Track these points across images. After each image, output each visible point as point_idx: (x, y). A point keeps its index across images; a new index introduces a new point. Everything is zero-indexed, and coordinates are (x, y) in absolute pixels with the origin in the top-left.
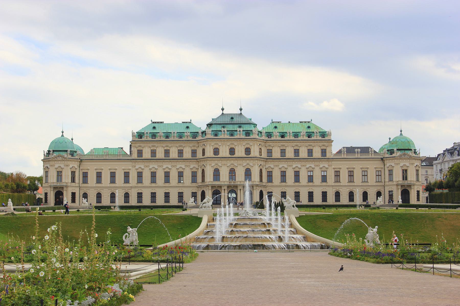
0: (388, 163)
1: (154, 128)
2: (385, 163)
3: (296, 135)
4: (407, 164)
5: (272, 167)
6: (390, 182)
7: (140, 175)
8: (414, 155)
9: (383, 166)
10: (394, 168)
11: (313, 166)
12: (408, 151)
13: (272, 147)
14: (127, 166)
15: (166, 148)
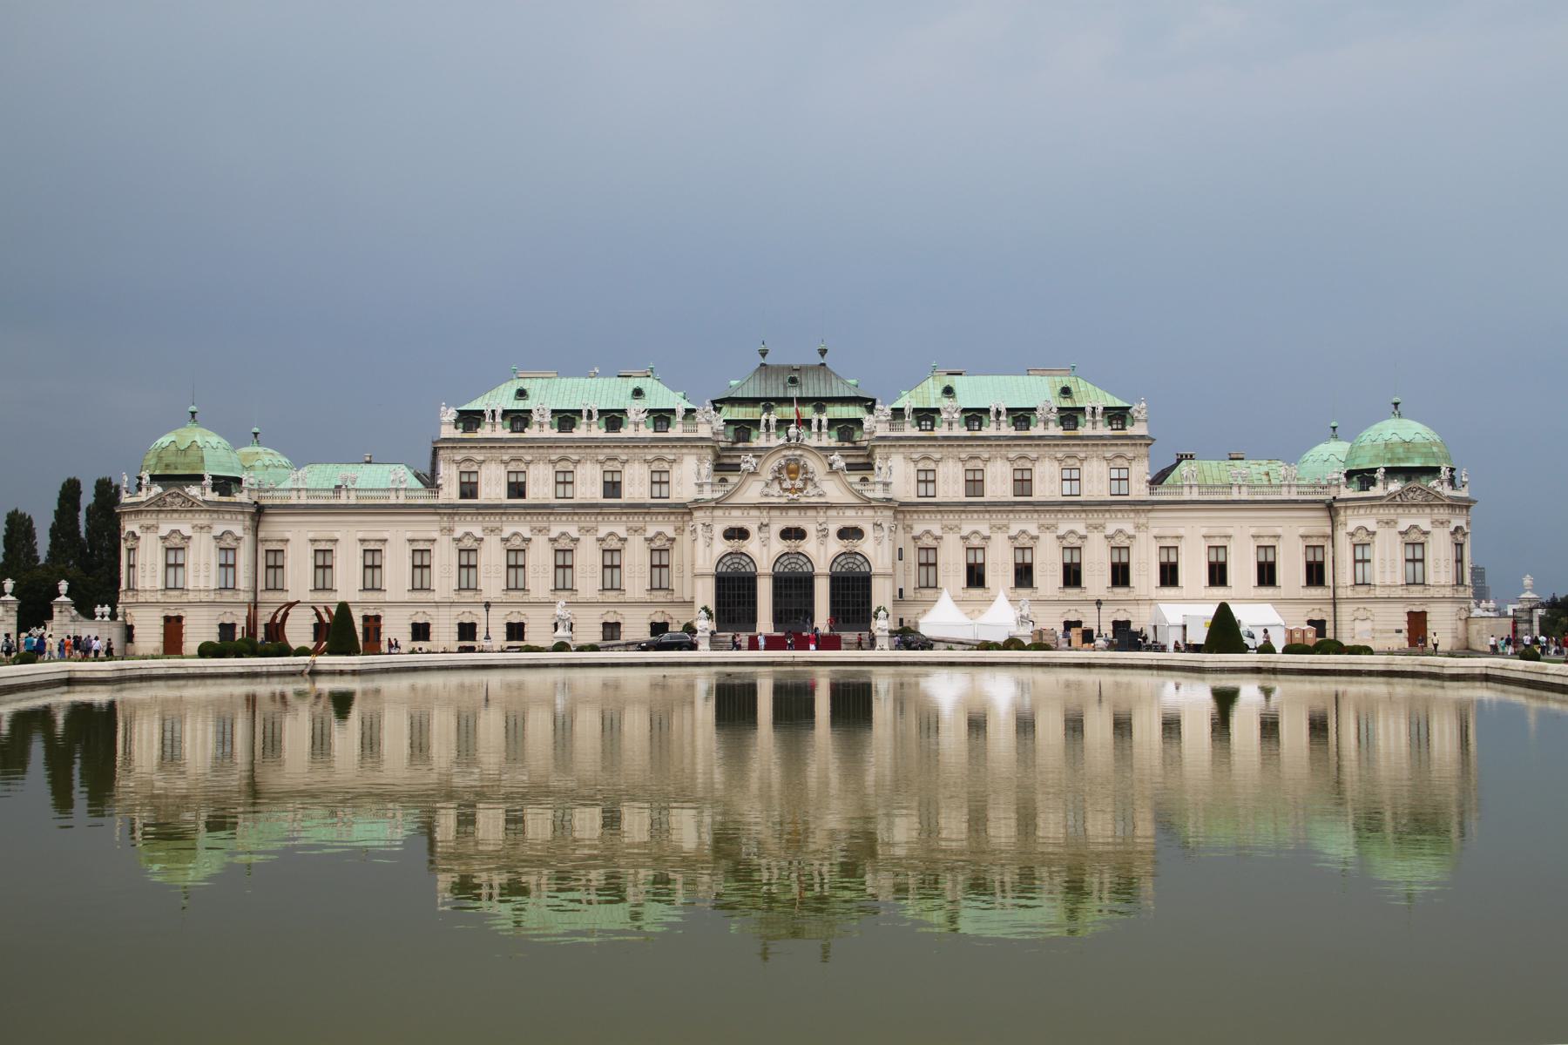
0: (1352, 521)
1: (521, 394)
2: (1341, 518)
3: (1021, 417)
4: (1425, 524)
5: (938, 532)
6: (1359, 589)
7: (467, 564)
8: (1447, 490)
9: (1329, 530)
10: (1377, 539)
11: (1081, 530)
12: (1424, 480)
13: (937, 462)
14: (427, 528)
15: (559, 467)
